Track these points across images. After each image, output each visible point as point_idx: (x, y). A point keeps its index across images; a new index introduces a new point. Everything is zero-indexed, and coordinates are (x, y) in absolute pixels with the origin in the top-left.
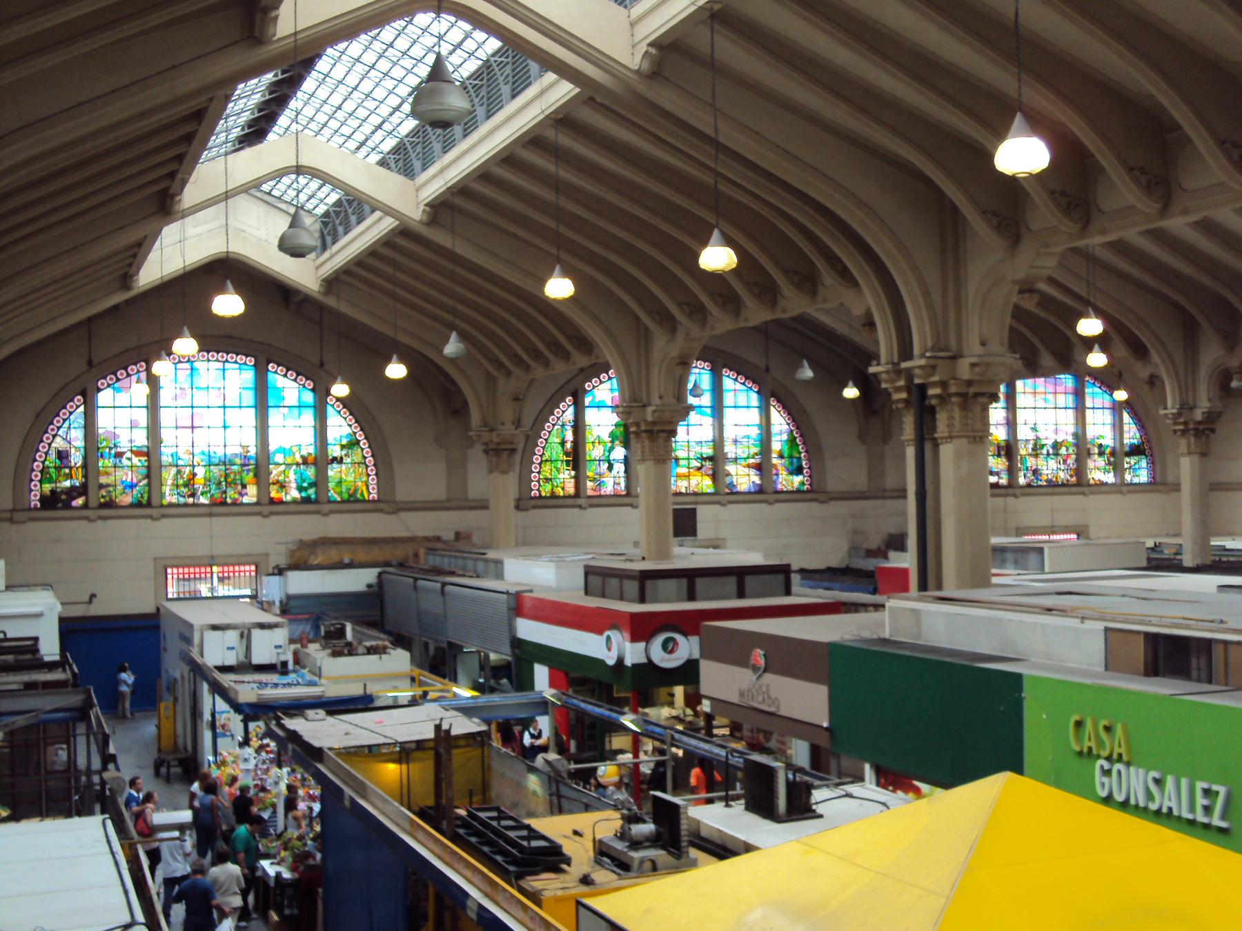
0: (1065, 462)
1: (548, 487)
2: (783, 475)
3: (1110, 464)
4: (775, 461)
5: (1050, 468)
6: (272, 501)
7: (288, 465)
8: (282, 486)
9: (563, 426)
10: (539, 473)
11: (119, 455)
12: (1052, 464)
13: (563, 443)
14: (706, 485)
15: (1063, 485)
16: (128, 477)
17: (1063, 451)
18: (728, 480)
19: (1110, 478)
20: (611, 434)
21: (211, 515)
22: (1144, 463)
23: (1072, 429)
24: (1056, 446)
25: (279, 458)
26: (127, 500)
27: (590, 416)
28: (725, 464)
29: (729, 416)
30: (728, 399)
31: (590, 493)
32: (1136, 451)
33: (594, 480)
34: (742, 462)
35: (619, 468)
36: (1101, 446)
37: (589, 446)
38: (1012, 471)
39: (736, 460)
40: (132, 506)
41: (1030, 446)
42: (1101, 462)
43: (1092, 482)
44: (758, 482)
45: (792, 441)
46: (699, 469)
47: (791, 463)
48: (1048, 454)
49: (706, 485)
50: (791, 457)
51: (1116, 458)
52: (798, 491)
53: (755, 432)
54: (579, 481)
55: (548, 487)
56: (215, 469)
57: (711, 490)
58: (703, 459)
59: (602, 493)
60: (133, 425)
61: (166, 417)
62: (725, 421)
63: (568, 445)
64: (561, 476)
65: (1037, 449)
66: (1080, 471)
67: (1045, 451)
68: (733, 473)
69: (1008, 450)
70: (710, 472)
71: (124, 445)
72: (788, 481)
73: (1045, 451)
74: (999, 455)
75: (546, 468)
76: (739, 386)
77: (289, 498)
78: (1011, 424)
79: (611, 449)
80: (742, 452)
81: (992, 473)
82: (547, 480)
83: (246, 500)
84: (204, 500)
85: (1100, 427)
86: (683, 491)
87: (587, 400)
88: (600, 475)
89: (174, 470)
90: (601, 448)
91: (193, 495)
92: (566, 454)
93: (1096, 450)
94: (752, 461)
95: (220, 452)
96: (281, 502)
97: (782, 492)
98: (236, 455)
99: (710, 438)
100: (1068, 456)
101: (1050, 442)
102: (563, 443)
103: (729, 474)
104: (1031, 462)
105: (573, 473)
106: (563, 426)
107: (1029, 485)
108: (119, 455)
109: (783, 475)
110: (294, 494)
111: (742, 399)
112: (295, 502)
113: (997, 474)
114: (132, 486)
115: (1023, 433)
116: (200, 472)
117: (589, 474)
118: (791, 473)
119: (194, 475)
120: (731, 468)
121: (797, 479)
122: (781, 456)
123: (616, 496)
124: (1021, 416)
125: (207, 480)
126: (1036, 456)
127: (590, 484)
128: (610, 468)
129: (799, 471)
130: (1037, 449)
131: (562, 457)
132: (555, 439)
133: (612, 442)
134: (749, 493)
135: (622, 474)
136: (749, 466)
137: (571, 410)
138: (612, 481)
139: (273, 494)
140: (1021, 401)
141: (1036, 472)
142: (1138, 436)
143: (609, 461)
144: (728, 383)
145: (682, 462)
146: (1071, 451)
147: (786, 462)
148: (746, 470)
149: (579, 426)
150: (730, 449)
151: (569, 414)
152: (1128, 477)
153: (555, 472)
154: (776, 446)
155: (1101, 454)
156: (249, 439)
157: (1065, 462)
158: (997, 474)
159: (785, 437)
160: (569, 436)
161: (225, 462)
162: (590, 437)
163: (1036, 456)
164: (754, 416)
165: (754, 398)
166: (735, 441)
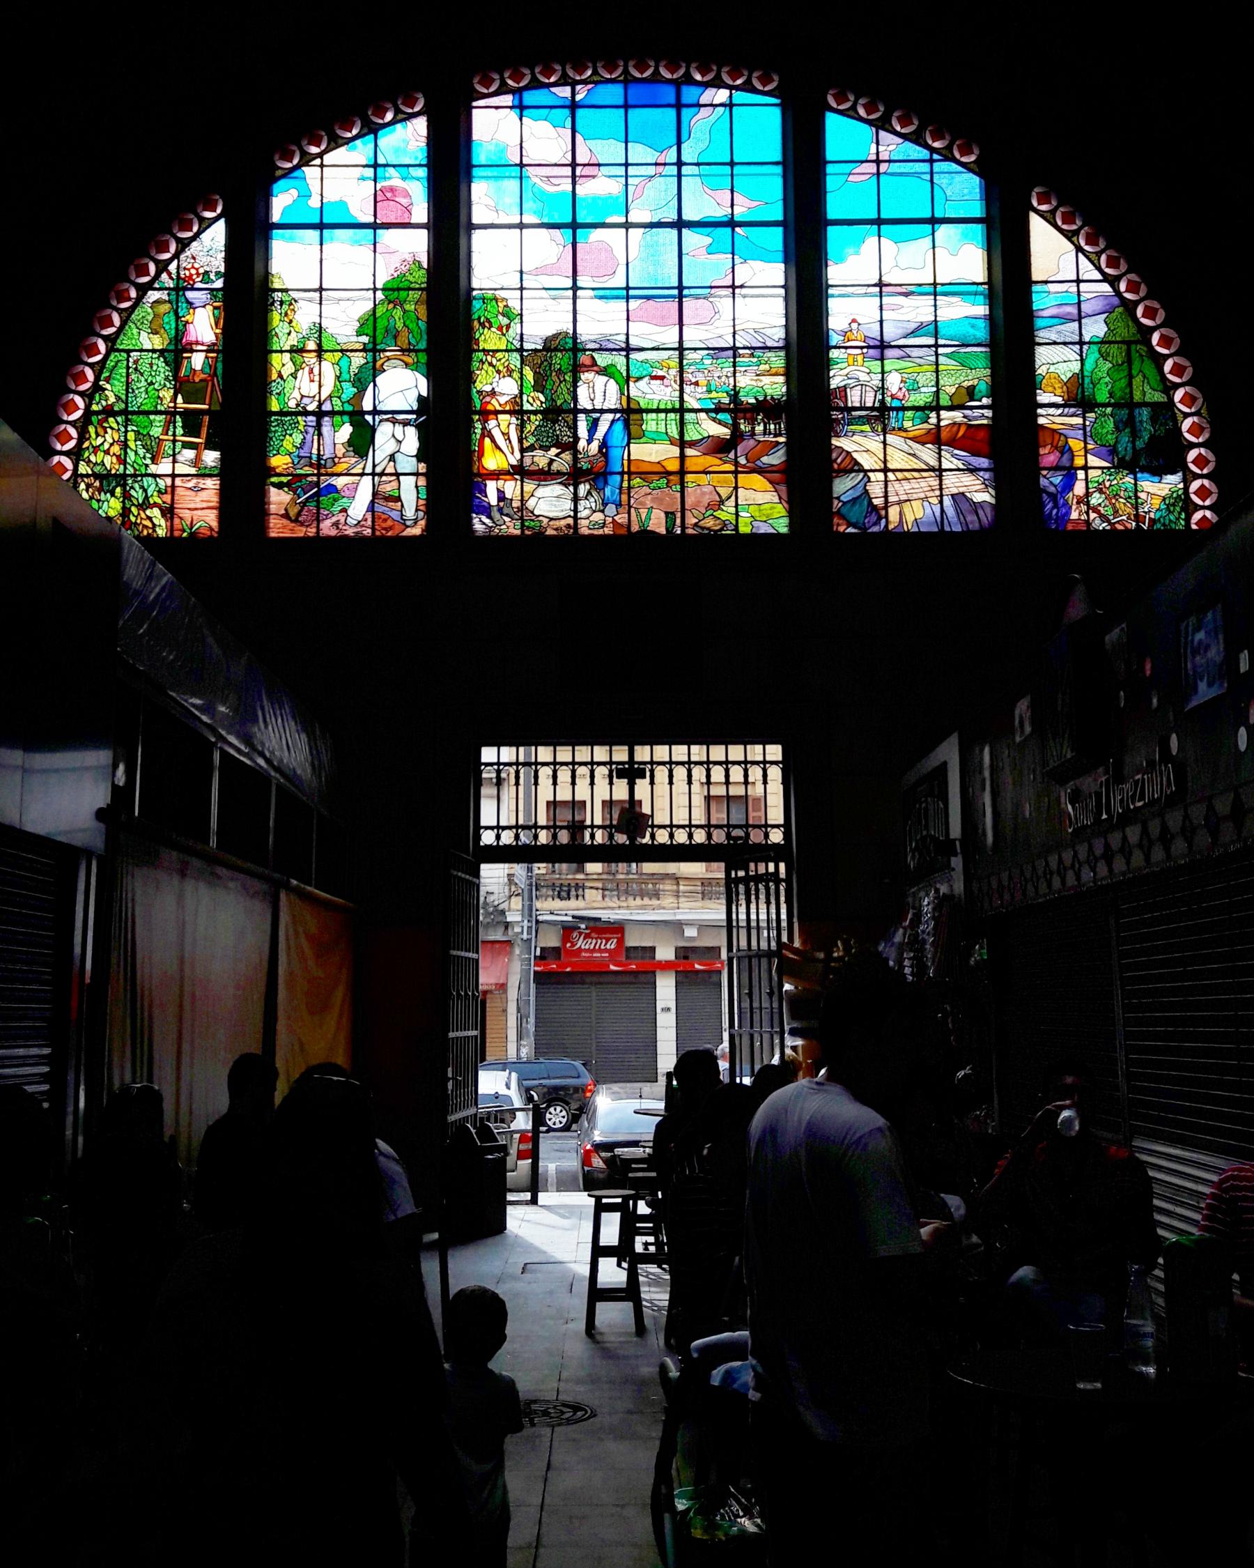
2: (1094, 467)
4: (1046, 418)
9: (181, 287)
10: (76, 454)
13: (177, 350)
14: (760, 507)
18: (843, 487)
20: (369, 323)
27: (290, 260)
28: (830, 428)
29: (850, 264)
30: (843, 195)
31: (277, 528)
33: (293, 483)
34: (909, 421)
35: (399, 444)
37: (280, 363)
39: (881, 416)
44: (984, 497)
46: (720, 447)
47: (1128, 424)
49: (760, 507)
50: (1125, 406)
53: (967, 314)
54: (243, 480)
57: (782, 526)
58: (736, 408)
59: (327, 528)
62: (834, 274)
63: (198, 361)
64: (164, 467)
68: (866, 462)
70: (776, 459)
75: (107, 438)
76: (892, 145)
82: (107, 481)
86: (657, 523)
87: (282, 202)
90: (328, 372)
92: (182, 384)
94: (948, 417)
99: (777, 334)
102: (177, 350)
103: (855, 467)
105: (211, 457)
111: (905, 195)
117: (278, 462)
120: (860, 445)
121: (1156, 490)
127: (278, 499)
128: (362, 442)
129: (1163, 455)
133: (373, 349)
135: (407, 463)
136: (936, 438)
138: (365, 489)
143: (356, 417)
144: (844, 136)
145: (651, 423)
148: (928, 454)
149: (248, 297)
150: (850, 374)
151: (210, 246)
153: (137, 454)
154: (1055, 362)
159: (1095, 328)
160: (204, 326)
162: (283, 335)
164: (966, 257)
165: (963, 189)
166: (881, 347)
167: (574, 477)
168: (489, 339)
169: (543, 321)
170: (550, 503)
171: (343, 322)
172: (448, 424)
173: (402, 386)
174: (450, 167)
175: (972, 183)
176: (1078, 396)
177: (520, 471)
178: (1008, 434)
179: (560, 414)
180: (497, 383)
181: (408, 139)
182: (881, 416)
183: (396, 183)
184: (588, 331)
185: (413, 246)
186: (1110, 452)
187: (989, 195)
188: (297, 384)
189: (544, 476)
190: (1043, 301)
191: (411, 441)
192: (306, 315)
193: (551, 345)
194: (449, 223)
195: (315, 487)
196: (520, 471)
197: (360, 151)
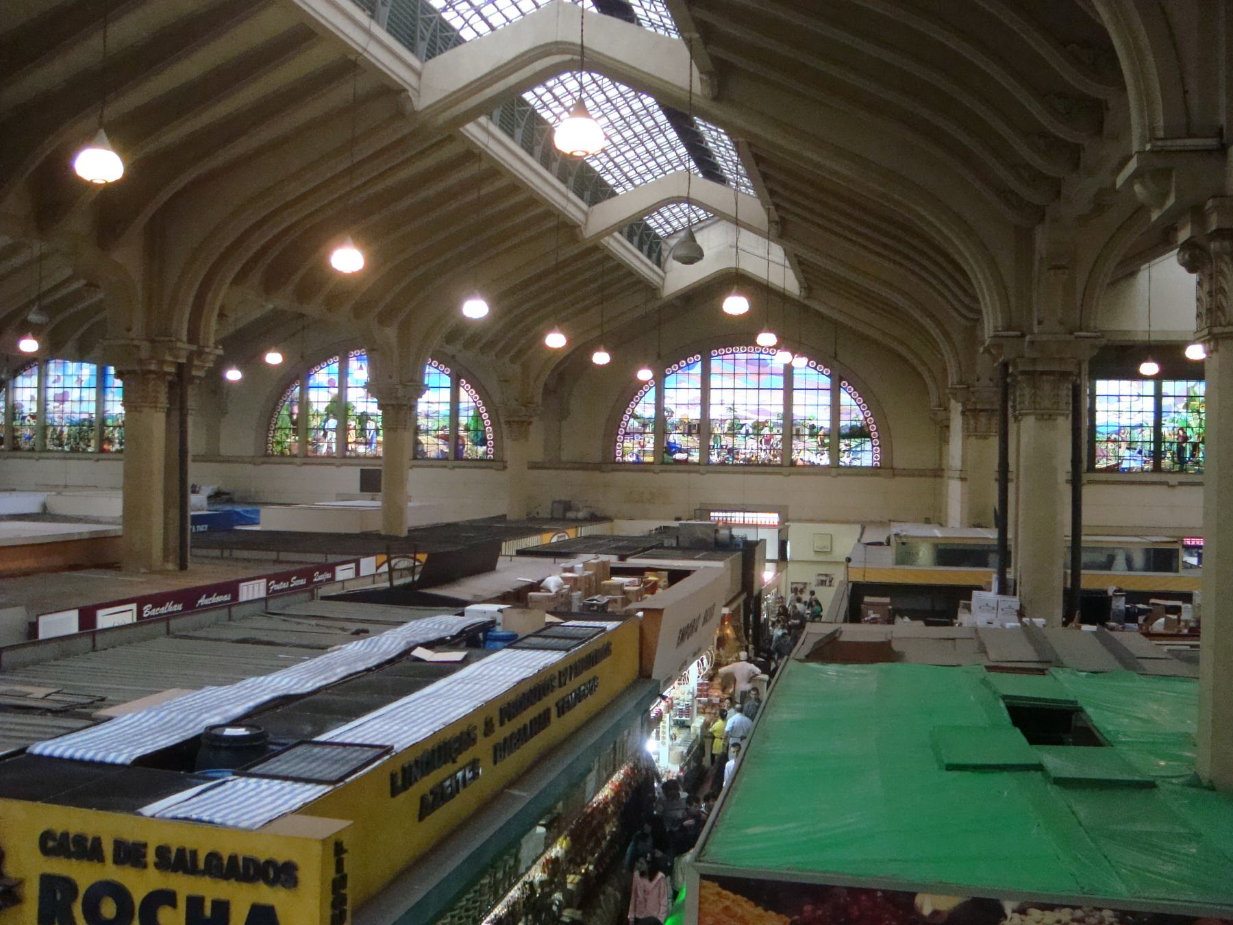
0: (767, 442)
1: (279, 448)
3: (823, 445)
5: (748, 447)
6: (102, 451)
7: (115, 427)
8: (110, 441)
11: (24, 418)
12: (752, 443)
15: (764, 465)
16: (28, 432)
17: (766, 431)
19: (825, 460)
20: (327, 409)
21: (65, 458)
22: (868, 446)
23: (781, 410)
24: (758, 426)
25: (109, 422)
26: (27, 447)
27: (313, 395)
32: (859, 433)
33: (313, 444)
35: (332, 435)
36: (813, 427)
38: (705, 450)
39: (427, 432)
40: (29, 450)
41: (727, 425)
42: (812, 443)
43: (800, 463)
45: (478, 416)
48: (747, 434)
50: (476, 430)
51: (835, 436)
52: (481, 460)
53: (445, 409)
54: (304, 442)
55: (279, 448)
56: (74, 428)
60: (32, 399)
61: (51, 394)
65: (734, 429)
66: (788, 449)
67: (743, 431)
69: (701, 429)
71: (26, 411)
72: (473, 450)
73: (743, 431)
74: (690, 434)
77: (113, 449)
78: (705, 403)
79: (326, 421)
80: (432, 424)
81: (680, 451)
82: (279, 443)
83: (90, 450)
84: (66, 448)
85: (813, 406)
87: (311, 382)
88: (318, 440)
89: (51, 429)
91: (61, 445)
92: (294, 423)
93: (807, 431)
94: (441, 433)
95: (76, 417)
96: (109, 451)
97: (467, 460)
98: (85, 420)
100: (772, 436)
101: (750, 422)
102: (291, 414)
104: (727, 441)
106: (292, 401)
107: (723, 464)
108: (24, 418)
109: (469, 445)
110: (117, 447)
112: (118, 451)
113: (687, 451)
114: (30, 438)
115: (715, 413)
116: (66, 430)
118: (476, 444)
119: (62, 432)
120: (423, 438)
121: (481, 450)
122: (467, 429)
123: (329, 456)
124: (715, 396)
125: (69, 435)
126: (734, 435)
128: (325, 435)
129: (483, 442)
130: (734, 429)
131: (290, 425)
132: (285, 412)
134: (438, 459)
136: (438, 437)
137: (298, 389)
139: (106, 447)
140: (715, 381)
141: (732, 451)
142: (861, 417)
146: (775, 431)
147: (472, 434)
148: (436, 440)
149: (305, 404)
152: (845, 460)
154: (463, 421)
155: (812, 435)
156: (92, 408)
157: (767, 442)
158: (687, 451)
159: (471, 413)
160: (296, 410)
161: (81, 423)
163: (734, 435)
164: (446, 395)
165: (446, 381)
166: (427, 416)
167: (366, 444)
168: (350, 413)
169: (360, 408)
170: (361, 449)
171: (322, 408)
172: (343, 430)
173: (332, 423)
174: (343, 373)
175: (448, 379)
176: (467, 429)
177: (355, 442)
178: (452, 437)
179: (363, 429)
180: (352, 423)
181: (335, 367)
182: (427, 432)
183: (332, 377)
184: (369, 411)
185: (335, 391)
186: (472, 441)
187: (452, 382)
188: (315, 422)
189: (360, 443)
190: (462, 406)
191: (334, 435)
192: (315, 407)
193: (363, 414)
194: (343, 386)
195: (316, 443)
196: (355, 442)
197: (325, 371)
